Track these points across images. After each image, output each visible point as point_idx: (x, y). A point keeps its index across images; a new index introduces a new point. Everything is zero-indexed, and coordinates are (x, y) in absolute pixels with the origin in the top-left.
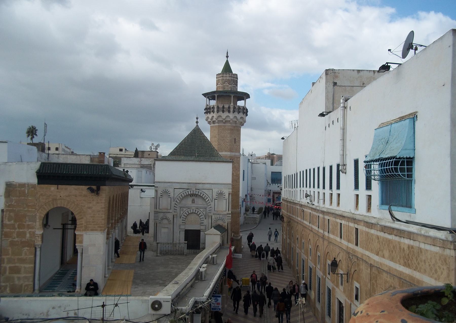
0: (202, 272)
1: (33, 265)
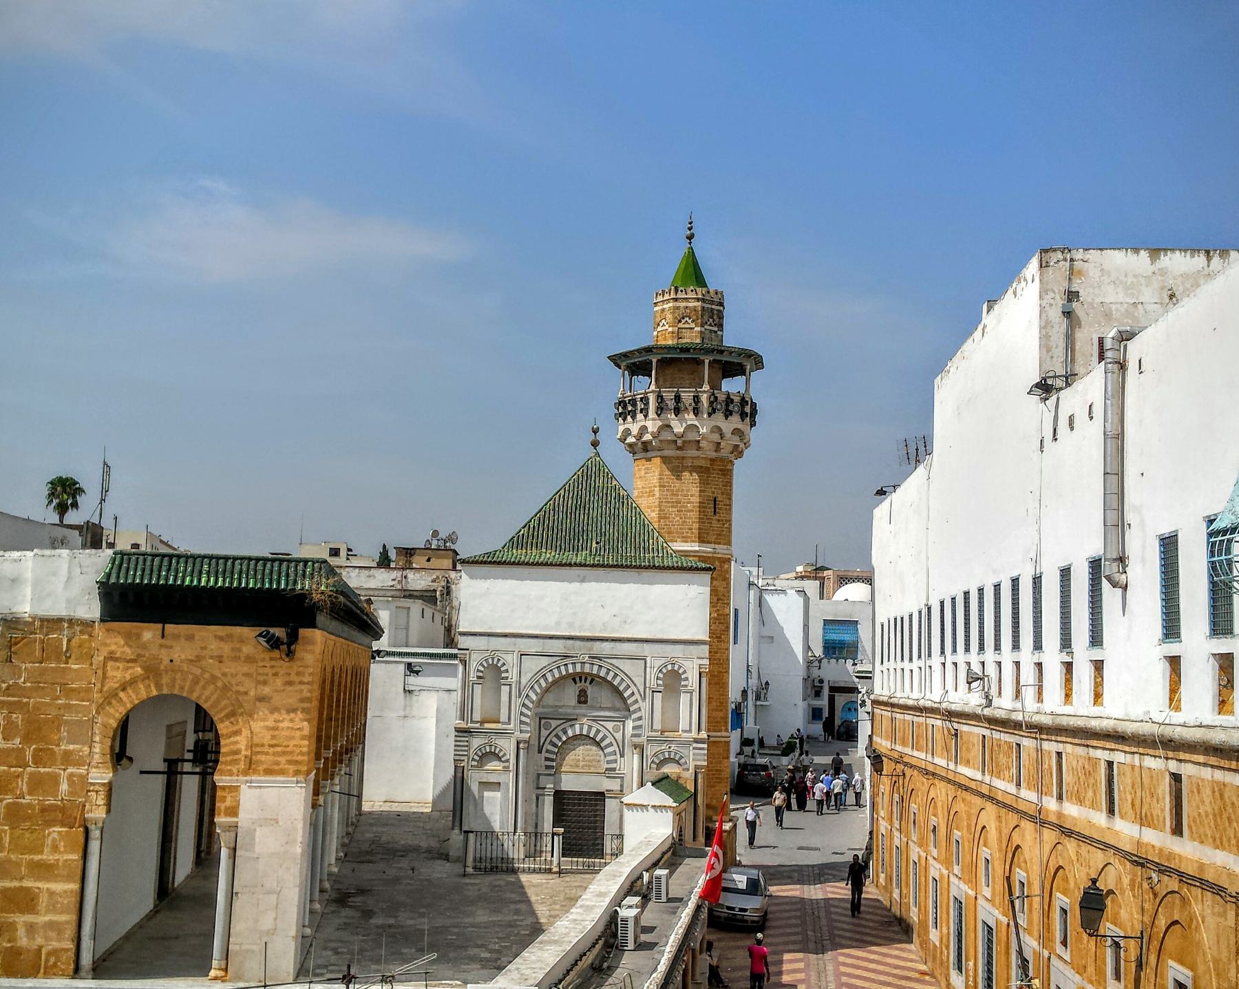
0: (625, 920)
1: (74, 886)
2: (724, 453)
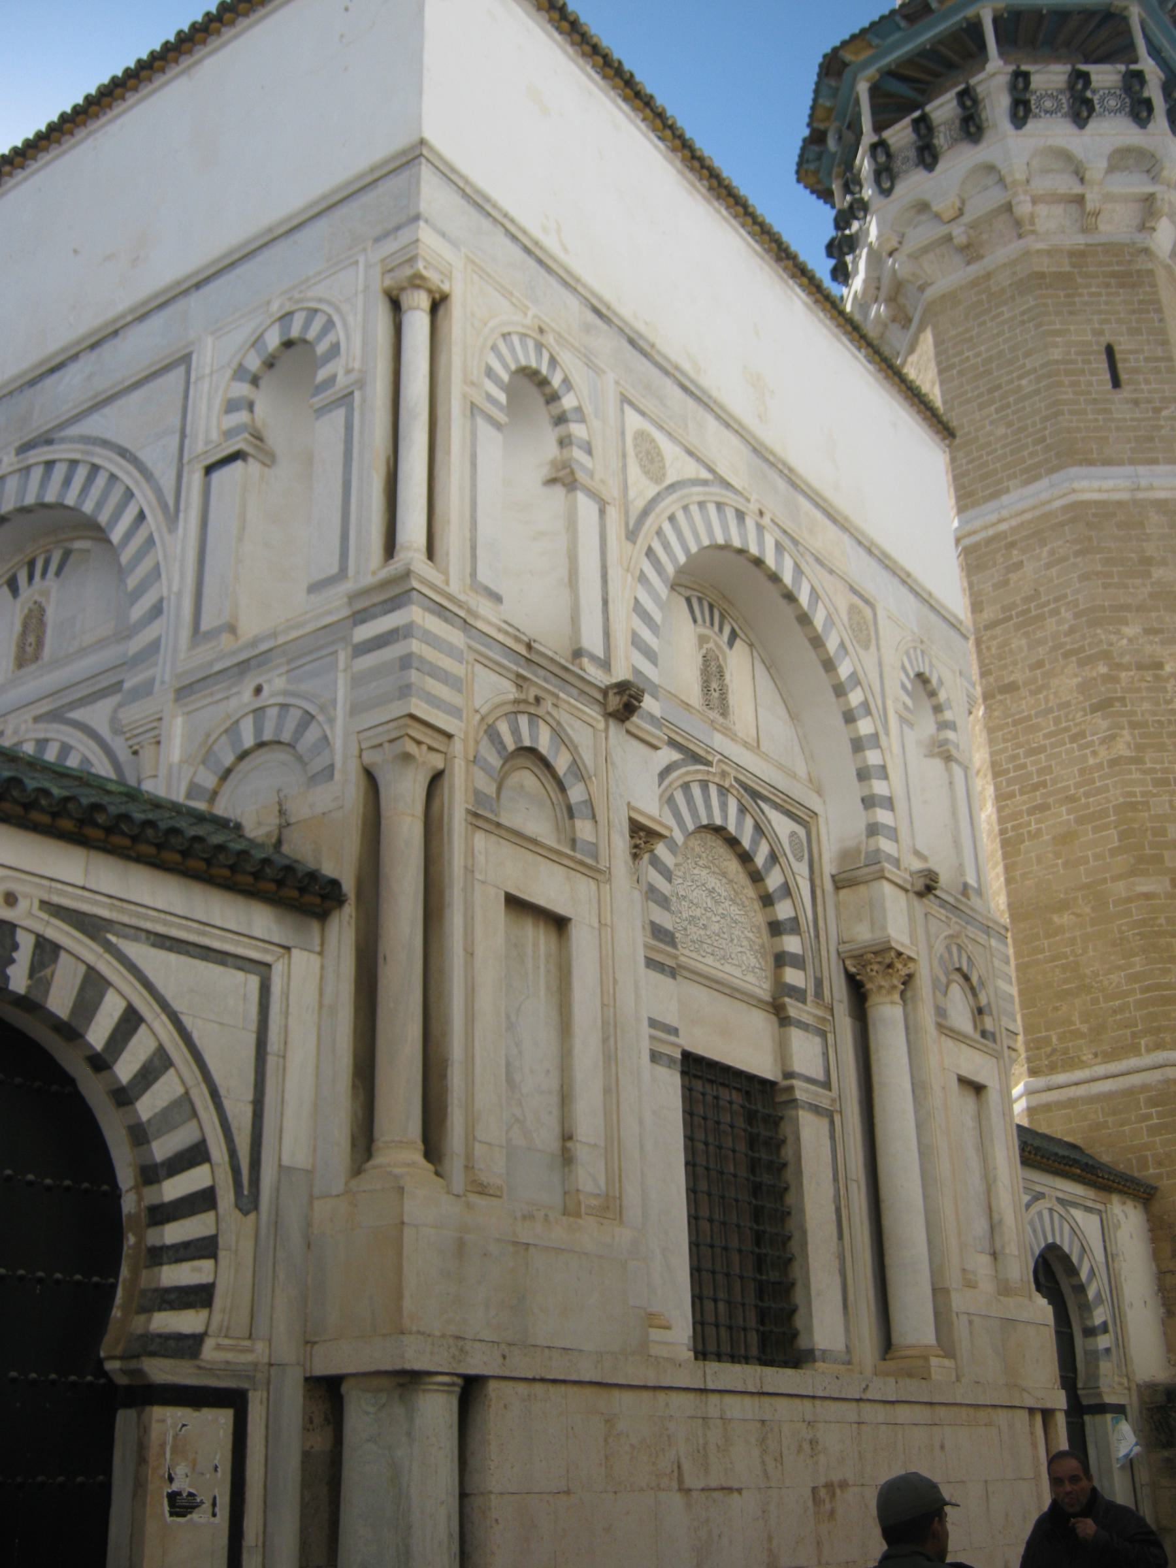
2: (1117, 224)
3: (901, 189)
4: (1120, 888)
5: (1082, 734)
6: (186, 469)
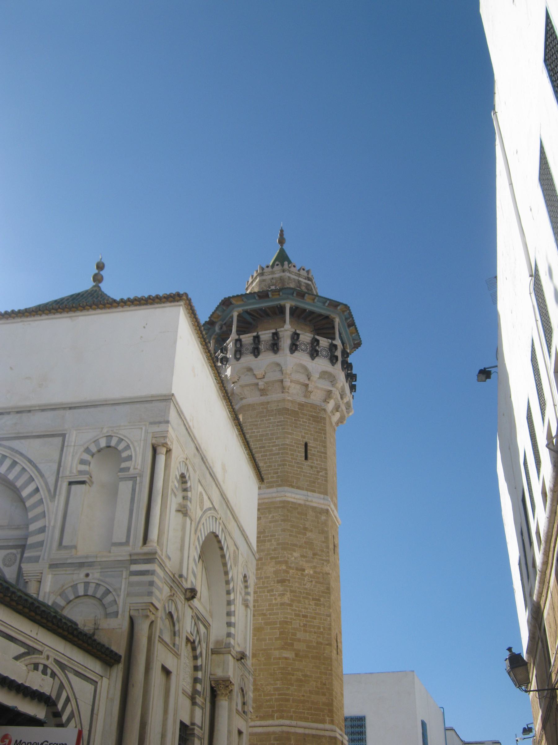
2: (316, 397)
3: (243, 360)
4: (276, 653)
5: (272, 590)
6: (60, 479)
